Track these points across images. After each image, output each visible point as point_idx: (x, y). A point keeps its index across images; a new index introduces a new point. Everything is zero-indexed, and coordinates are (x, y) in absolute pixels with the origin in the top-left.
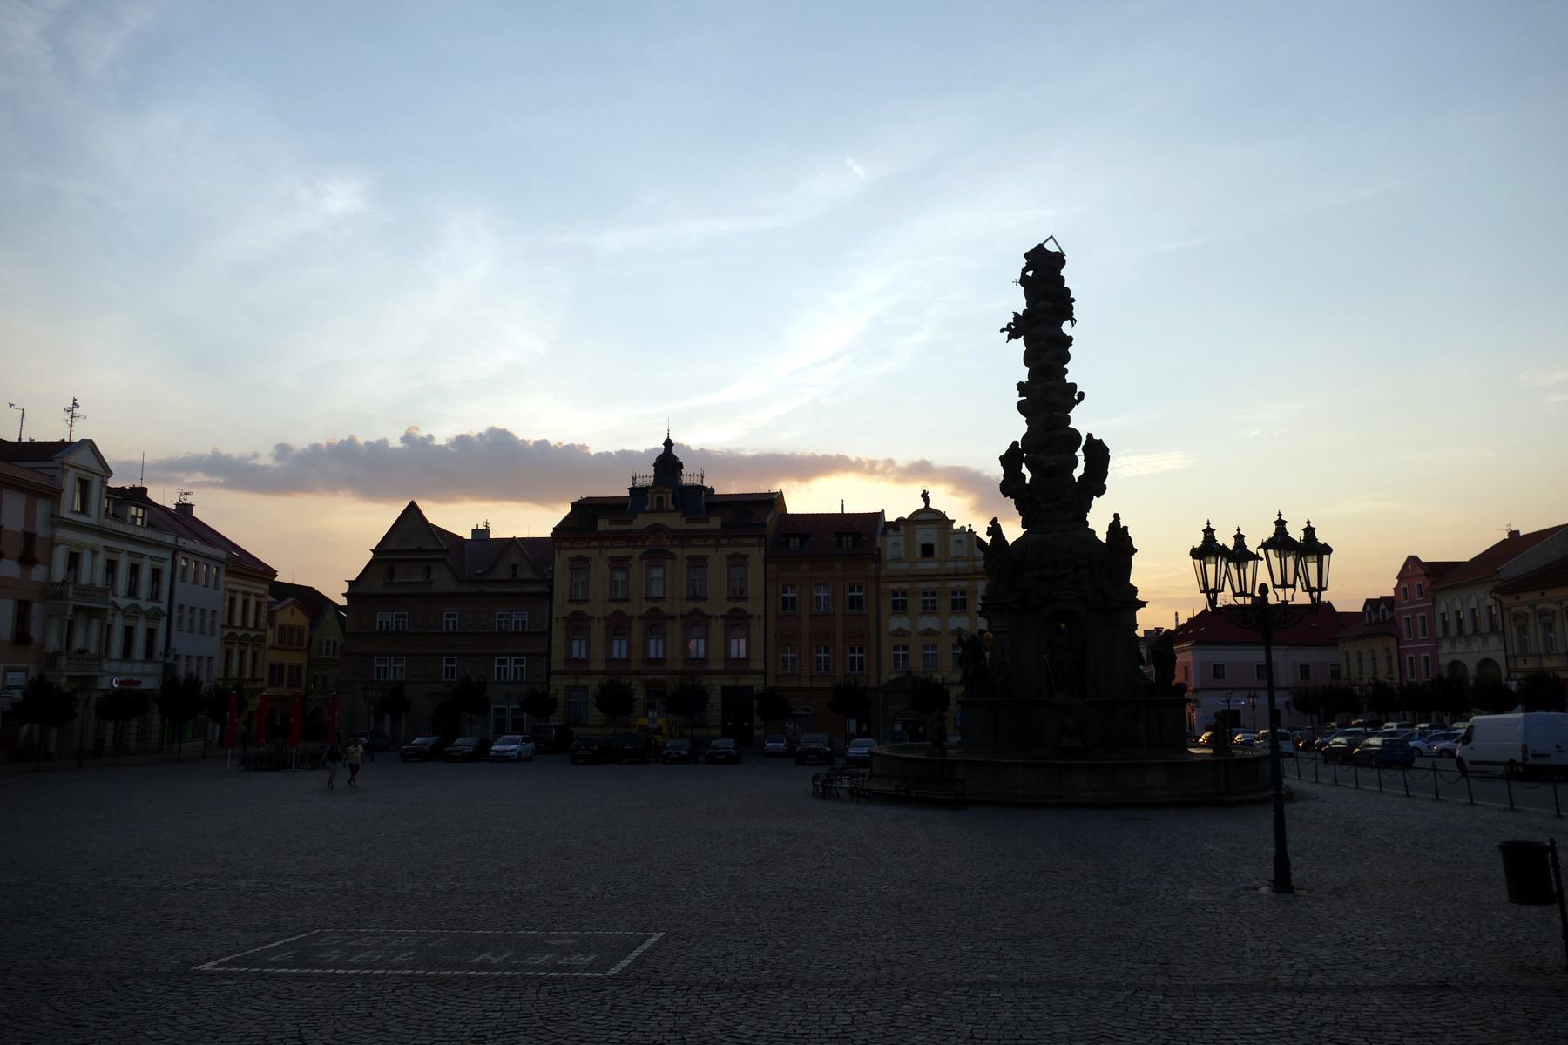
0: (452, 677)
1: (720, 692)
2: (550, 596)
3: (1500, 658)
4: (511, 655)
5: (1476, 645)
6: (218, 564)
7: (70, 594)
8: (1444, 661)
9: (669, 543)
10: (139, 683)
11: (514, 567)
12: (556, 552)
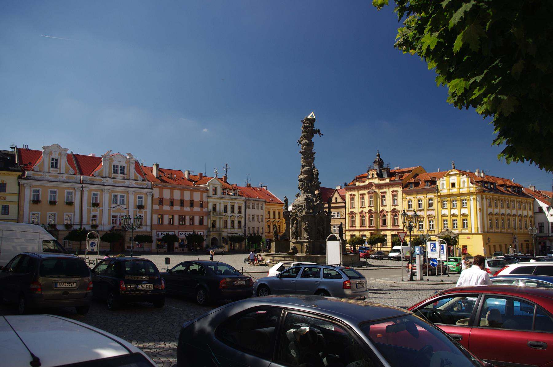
1: (390, 236)
2: (345, 207)
6: (262, 203)
7: (211, 214)
9: (375, 188)
10: (237, 233)
11: (336, 198)
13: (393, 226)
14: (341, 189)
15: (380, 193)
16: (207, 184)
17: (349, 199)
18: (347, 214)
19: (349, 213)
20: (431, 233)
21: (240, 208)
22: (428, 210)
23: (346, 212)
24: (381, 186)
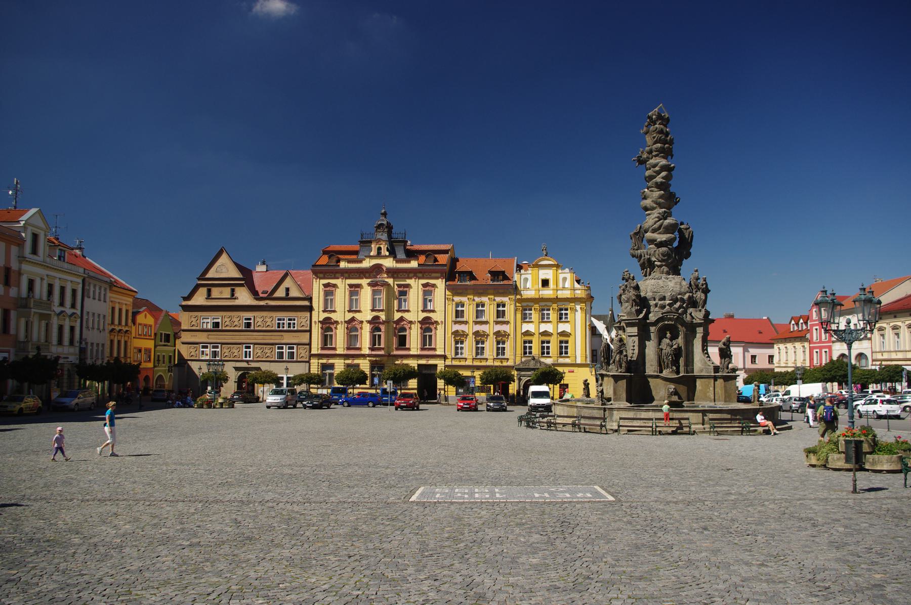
0: (250, 357)
2: (310, 309)
4: (286, 344)
6: (104, 286)
7: (32, 306)
10: (67, 358)
11: (287, 290)
12: (314, 280)
13: (322, 349)
14: (267, 271)
15: (396, 287)
16: (22, 223)
17: (322, 293)
18: (315, 322)
19: (319, 321)
20: (502, 362)
21: (74, 292)
22: (497, 323)
23: (313, 318)
24: (399, 272)
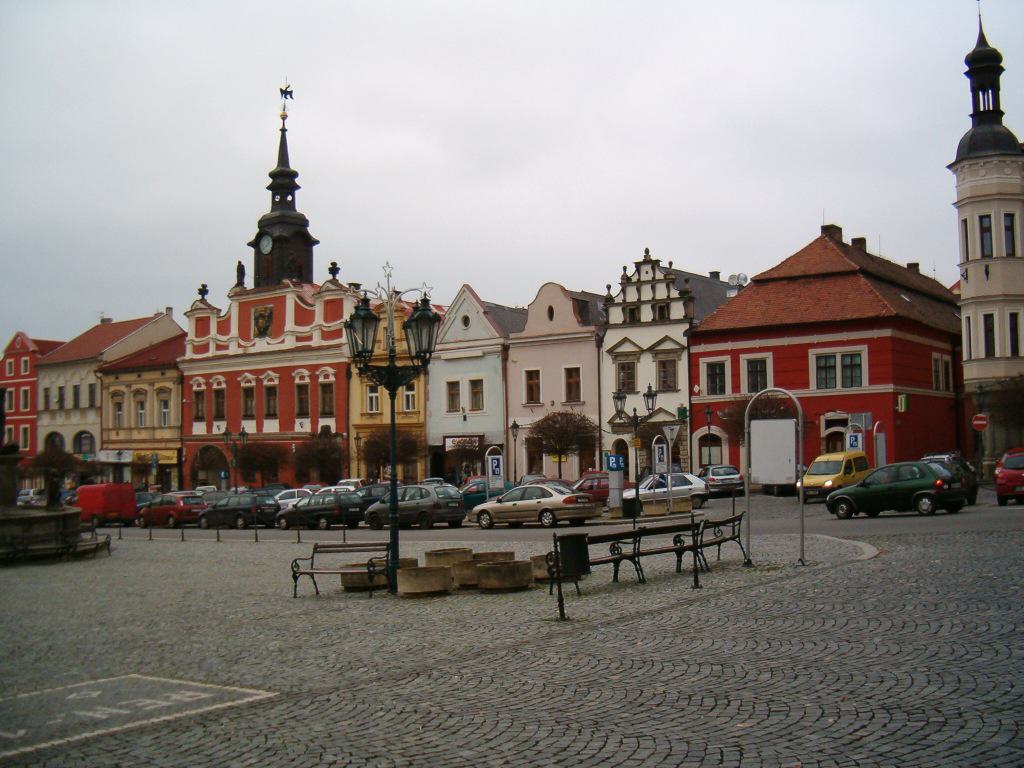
3: (96, 432)
5: (75, 418)
8: (42, 435)
